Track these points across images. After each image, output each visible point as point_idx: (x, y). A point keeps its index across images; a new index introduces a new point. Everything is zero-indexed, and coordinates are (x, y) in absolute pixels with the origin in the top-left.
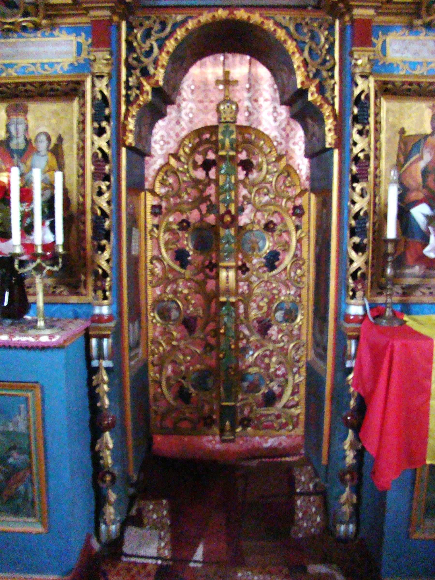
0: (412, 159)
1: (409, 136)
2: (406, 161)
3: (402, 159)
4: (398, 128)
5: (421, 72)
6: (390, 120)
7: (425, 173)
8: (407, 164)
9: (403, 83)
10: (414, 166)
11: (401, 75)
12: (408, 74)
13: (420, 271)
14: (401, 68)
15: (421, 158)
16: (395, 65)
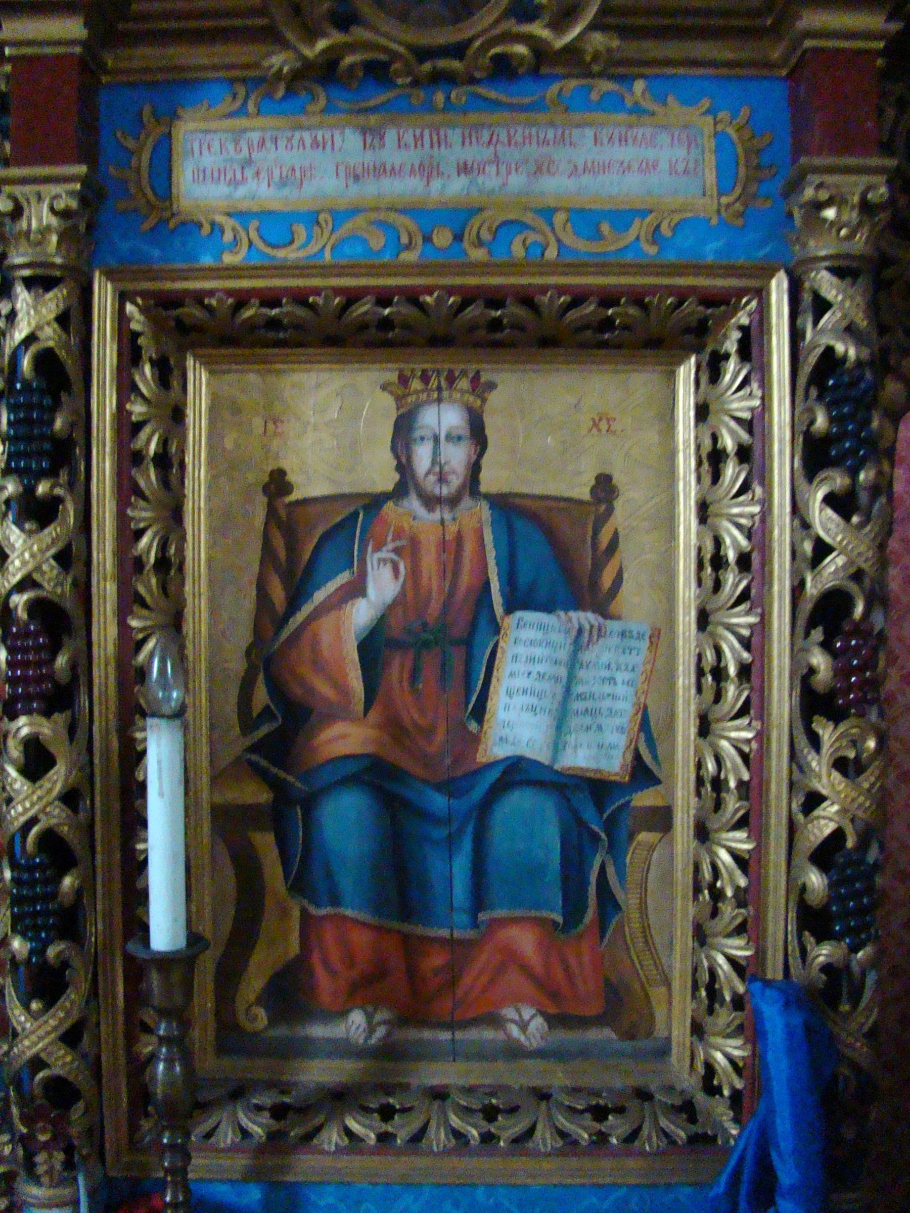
0: (319, 596)
1: (306, 502)
2: (293, 605)
3: (278, 593)
4: (257, 476)
5: (314, 248)
6: (229, 444)
7: (373, 647)
8: (300, 617)
9: (242, 299)
10: (326, 624)
11: (225, 263)
12: (256, 261)
13: (371, 1029)
14: (228, 236)
15: (357, 589)
16: (206, 229)
